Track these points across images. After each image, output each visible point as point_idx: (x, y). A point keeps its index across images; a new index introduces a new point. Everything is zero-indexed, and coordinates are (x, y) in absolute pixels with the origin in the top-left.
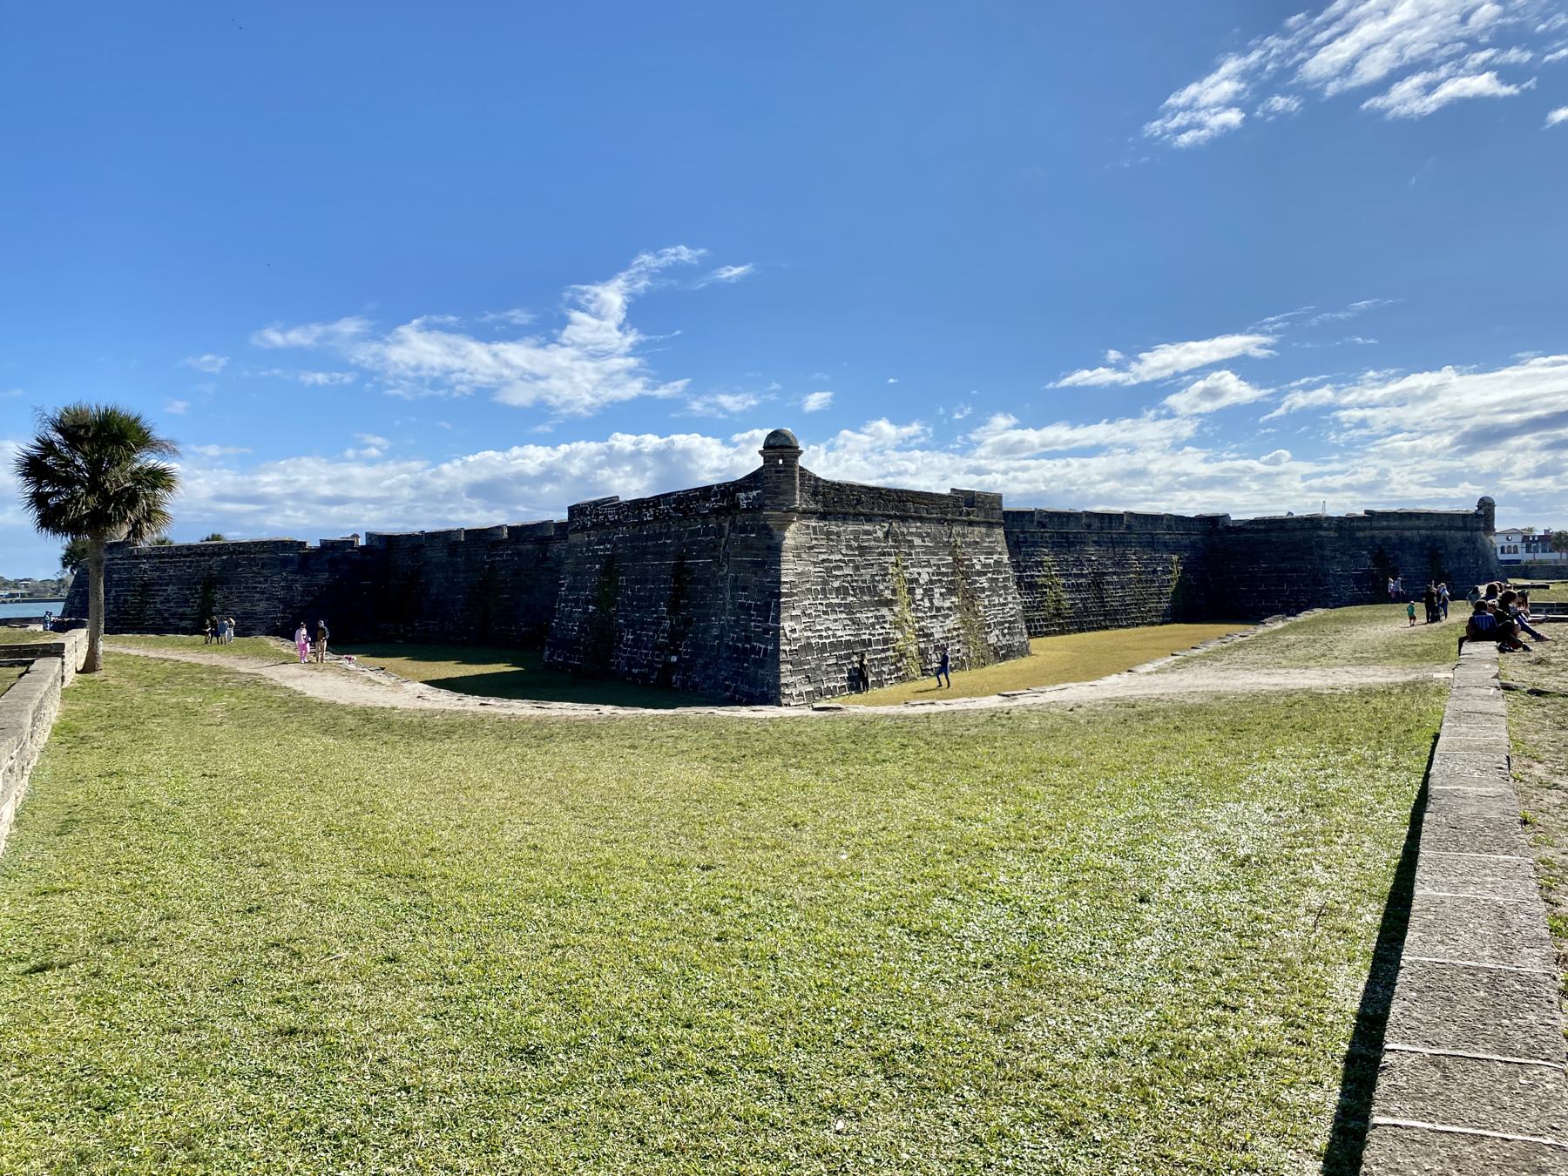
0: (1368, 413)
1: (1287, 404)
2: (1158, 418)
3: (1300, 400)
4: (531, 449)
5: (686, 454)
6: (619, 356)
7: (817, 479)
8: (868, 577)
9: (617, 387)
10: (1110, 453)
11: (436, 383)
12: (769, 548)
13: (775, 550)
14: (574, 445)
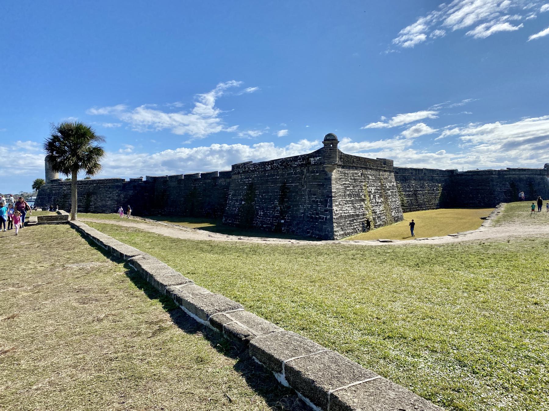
0: (471, 137)
1: (444, 134)
2: (400, 139)
3: (448, 133)
4: (183, 149)
5: (237, 151)
6: (213, 118)
7: (342, 153)
9: (213, 128)
11: (150, 127)
12: (325, 179)
13: (330, 179)
14: (199, 148)
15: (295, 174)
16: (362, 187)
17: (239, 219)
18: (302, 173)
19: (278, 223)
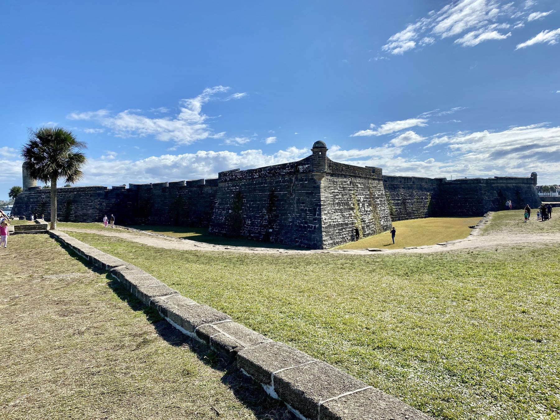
0: (460, 146)
1: (432, 142)
2: (389, 147)
3: (437, 141)
5: (224, 158)
6: (199, 124)
7: (330, 161)
8: (346, 199)
10: (373, 159)
11: (134, 133)
12: (314, 187)
13: (319, 188)
14: (184, 155)
15: (284, 182)
16: (351, 196)
17: (226, 228)
18: (290, 181)
19: (266, 232)
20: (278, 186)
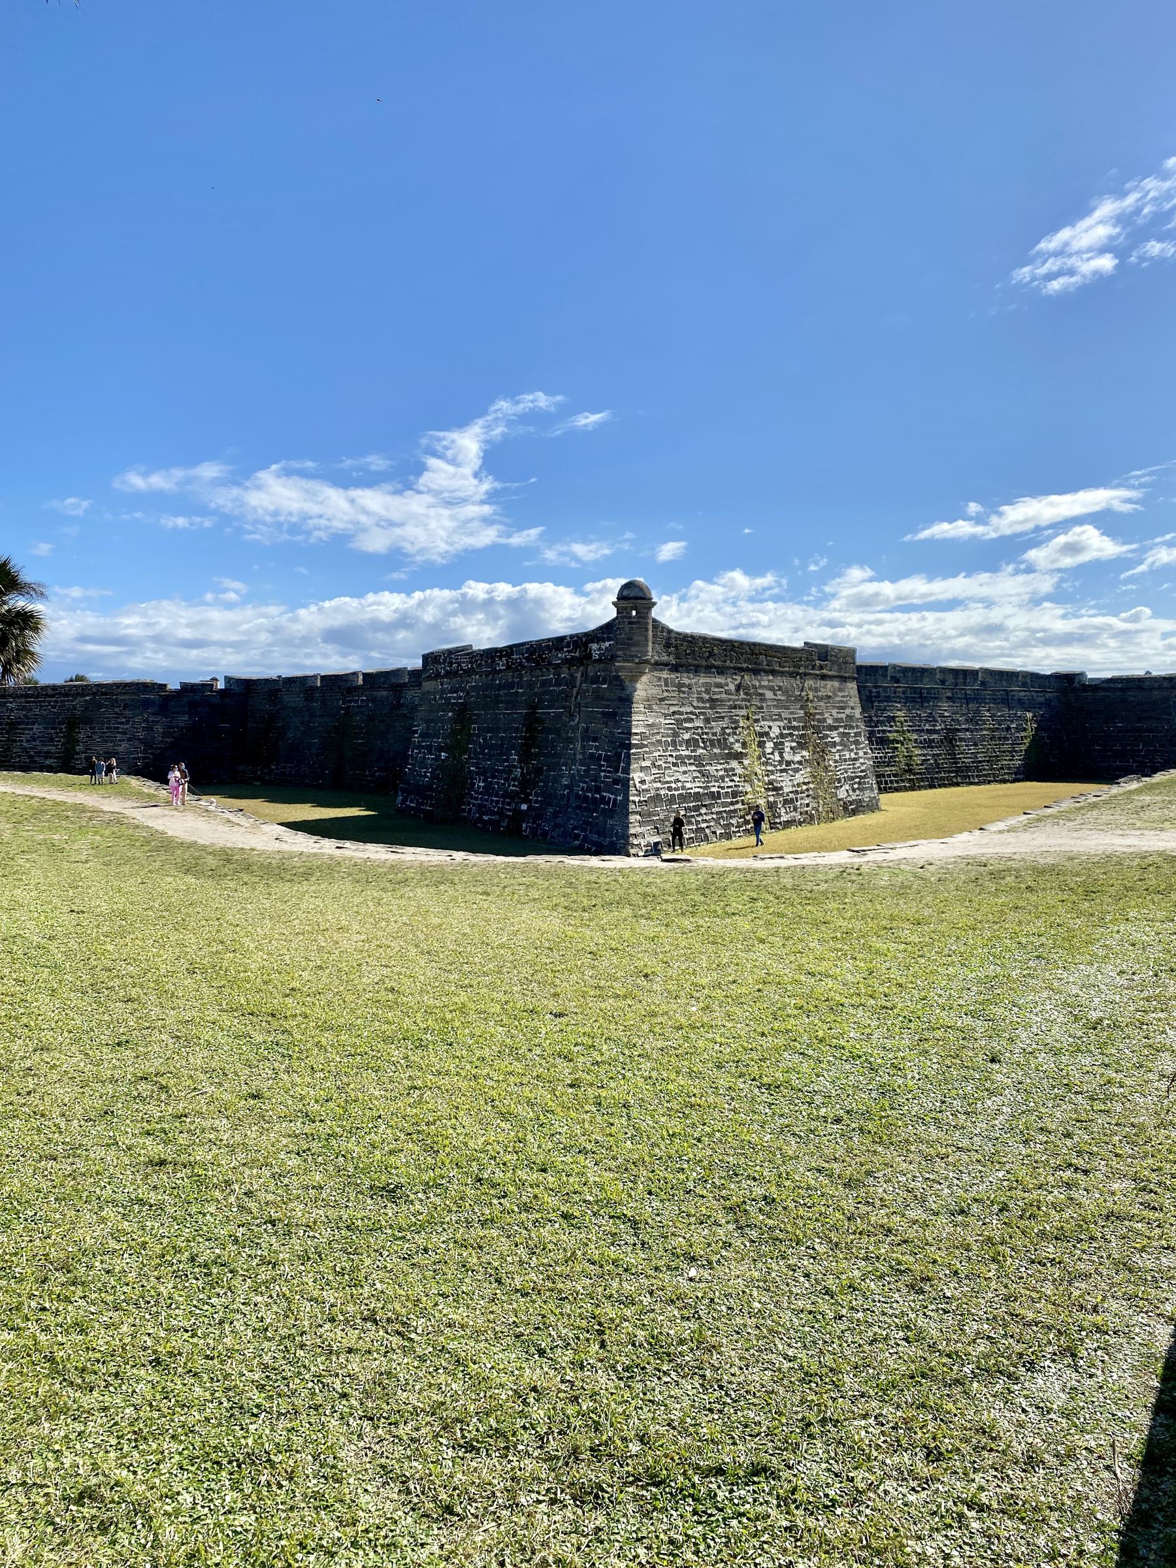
2: (1017, 572)
4: (386, 596)
5: (539, 602)
6: (474, 503)
8: (718, 730)
9: (471, 534)
10: (966, 607)
11: (294, 529)
12: (620, 699)
14: (428, 592)
16: (737, 722)
20: (546, 693)
